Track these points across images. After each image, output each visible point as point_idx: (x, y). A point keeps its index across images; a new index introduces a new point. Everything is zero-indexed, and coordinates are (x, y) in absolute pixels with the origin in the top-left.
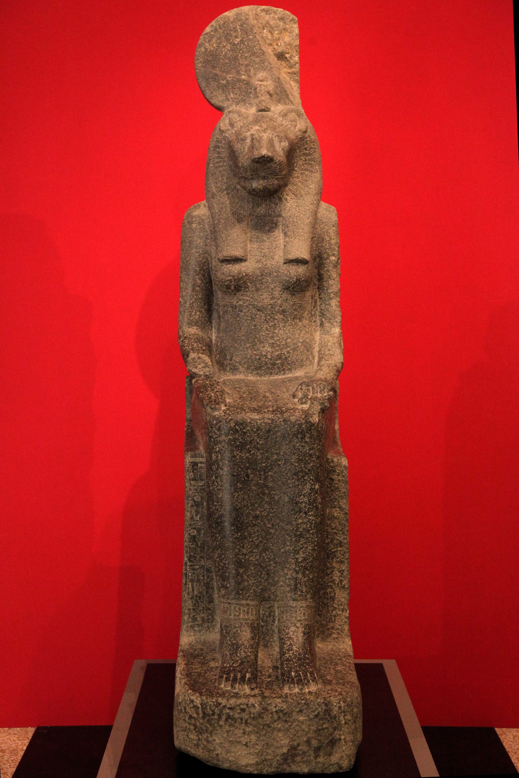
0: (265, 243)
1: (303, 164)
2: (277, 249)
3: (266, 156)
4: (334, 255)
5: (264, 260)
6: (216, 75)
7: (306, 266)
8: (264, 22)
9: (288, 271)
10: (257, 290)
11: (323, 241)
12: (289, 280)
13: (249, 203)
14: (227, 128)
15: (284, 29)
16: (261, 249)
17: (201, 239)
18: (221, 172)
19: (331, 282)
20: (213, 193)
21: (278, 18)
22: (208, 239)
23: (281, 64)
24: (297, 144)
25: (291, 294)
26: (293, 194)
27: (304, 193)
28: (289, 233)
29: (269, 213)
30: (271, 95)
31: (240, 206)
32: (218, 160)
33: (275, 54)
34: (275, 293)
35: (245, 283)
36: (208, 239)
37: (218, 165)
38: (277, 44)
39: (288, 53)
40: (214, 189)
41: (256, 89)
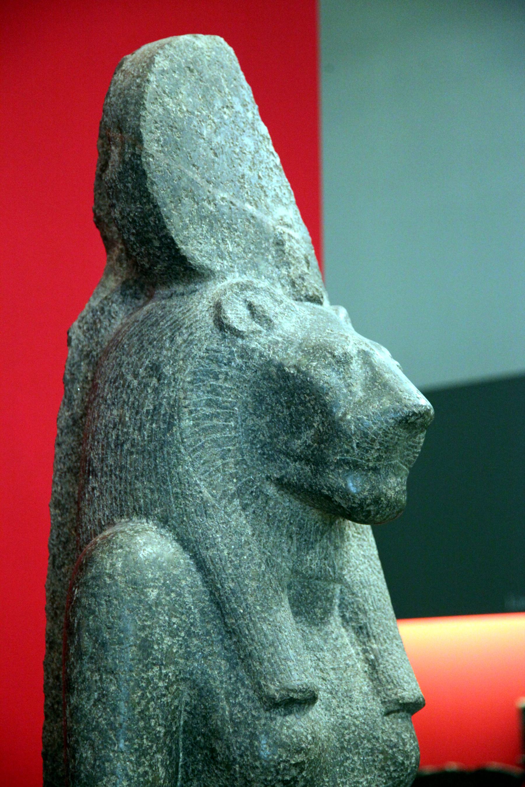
13: (291, 537)
17: (173, 634)
18: (219, 446)
20: (204, 502)
22: (197, 636)
28: (374, 629)
29: (325, 571)
31: (274, 545)
32: (208, 411)
36: (197, 636)
37: (208, 423)
40: (204, 490)
41: (279, 243)
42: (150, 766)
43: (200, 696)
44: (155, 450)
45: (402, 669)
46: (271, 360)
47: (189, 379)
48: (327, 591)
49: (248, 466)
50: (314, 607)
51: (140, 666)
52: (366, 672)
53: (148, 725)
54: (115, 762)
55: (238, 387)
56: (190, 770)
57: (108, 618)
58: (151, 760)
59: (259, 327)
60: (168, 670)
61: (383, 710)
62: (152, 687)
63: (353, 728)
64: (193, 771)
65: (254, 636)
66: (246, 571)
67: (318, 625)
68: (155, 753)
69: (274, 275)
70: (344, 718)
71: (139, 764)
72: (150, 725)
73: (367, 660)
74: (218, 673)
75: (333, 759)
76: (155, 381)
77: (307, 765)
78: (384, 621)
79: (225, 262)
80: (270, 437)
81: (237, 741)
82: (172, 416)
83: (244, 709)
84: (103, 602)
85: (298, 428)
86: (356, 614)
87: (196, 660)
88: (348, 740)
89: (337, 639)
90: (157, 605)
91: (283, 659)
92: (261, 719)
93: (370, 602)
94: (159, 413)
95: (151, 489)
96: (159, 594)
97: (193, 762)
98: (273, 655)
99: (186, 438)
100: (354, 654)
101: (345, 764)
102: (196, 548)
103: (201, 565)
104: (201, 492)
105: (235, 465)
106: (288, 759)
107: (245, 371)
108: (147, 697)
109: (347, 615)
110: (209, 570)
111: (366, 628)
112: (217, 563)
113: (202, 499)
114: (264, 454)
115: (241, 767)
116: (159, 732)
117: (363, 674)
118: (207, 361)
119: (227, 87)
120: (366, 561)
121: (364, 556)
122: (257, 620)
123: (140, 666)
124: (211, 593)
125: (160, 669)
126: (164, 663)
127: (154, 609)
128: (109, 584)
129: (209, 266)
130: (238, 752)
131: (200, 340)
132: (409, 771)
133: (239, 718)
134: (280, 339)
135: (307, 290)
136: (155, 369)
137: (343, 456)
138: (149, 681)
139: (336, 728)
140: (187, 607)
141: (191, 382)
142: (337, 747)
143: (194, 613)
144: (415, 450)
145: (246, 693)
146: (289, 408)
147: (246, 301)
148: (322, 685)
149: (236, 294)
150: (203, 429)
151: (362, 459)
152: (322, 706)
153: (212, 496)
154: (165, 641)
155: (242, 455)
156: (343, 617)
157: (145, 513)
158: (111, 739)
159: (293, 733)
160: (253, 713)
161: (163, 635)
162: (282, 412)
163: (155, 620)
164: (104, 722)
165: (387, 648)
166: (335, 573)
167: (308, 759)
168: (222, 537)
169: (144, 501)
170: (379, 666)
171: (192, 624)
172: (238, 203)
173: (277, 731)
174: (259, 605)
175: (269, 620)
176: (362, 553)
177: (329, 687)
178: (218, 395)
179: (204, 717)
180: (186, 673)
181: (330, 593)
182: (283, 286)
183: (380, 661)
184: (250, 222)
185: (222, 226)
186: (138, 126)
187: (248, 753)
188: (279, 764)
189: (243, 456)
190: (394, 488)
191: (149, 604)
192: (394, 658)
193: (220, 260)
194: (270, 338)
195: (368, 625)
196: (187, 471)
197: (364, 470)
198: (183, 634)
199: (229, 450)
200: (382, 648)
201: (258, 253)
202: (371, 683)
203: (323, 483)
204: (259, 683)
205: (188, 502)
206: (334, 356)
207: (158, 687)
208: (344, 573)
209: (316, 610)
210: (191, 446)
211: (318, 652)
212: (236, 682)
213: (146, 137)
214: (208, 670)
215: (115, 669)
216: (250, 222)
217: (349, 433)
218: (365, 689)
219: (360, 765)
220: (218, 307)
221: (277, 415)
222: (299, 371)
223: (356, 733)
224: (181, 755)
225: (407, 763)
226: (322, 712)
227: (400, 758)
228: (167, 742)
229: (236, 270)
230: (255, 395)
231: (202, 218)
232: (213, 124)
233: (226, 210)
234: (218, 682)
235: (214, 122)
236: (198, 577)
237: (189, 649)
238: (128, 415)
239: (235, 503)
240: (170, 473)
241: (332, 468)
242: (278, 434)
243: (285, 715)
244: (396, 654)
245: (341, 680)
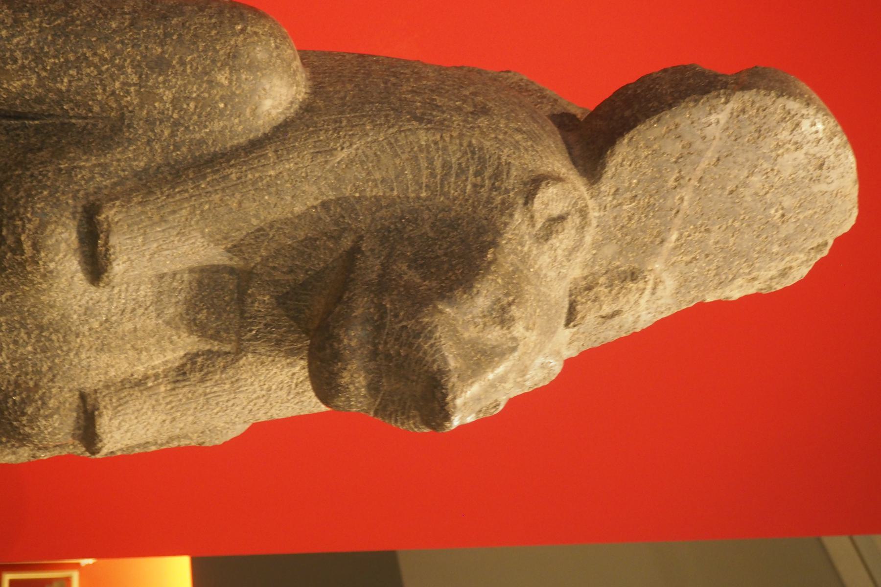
2: (131, 353)
5: (96, 325)
9: (57, 410)
12: (24, 414)
13: (291, 271)
14: (537, 215)
17: (175, 101)
18: (397, 177)
20: (331, 152)
22: (173, 135)
27: (302, 399)
29: (251, 324)
32: (438, 163)
41: (634, 275)
42: (23, 67)
43: (104, 138)
44: (389, 103)
45: (136, 421)
46: (501, 235)
47: (474, 141)
48: (227, 330)
49: (374, 213)
50: (208, 308)
51: (138, 58)
52: (132, 375)
53: (70, 65)
54: (29, 23)
55: (467, 200)
56: (18, 132)
57: (196, 24)
58: (30, 69)
59: (539, 225)
60: (133, 94)
61: (87, 391)
62: (114, 72)
63: (65, 349)
64: (18, 135)
65: (173, 197)
66: (250, 196)
67: (188, 314)
68: (39, 75)
69: (597, 267)
70: (77, 336)
71: (26, 51)
72: (70, 68)
73: (146, 377)
74: (129, 158)
75: (28, 311)
76: (471, 109)
77: (18, 257)
78: (194, 405)
80: (409, 238)
81: (49, 171)
82: (430, 122)
83: (87, 182)
84: (213, 21)
85: (422, 265)
86: (201, 370)
87: (145, 132)
89: (171, 342)
90: (210, 82)
91: (145, 231)
92: (75, 200)
93: (216, 389)
94: (434, 110)
95: (345, 97)
96: (222, 86)
97: (28, 135)
98: (150, 218)
99: (406, 136)
100: (153, 364)
101: (22, 330)
102: (276, 140)
103: (256, 145)
104: (343, 149)
105: (375, 197)
106: (27, 231)
107: (486, 207)
108: (103, 65)
109: (200, 360)
110: (251, 152)
111: (184, 380)
112: (259, 161)
113: (336, 149)
114: (389, 232)
115: (18, 176)
116: (62, 82)
117: (130, 371)
118: (496, 163)
119: (805, 217)
120: (264, 392)
121: (269, 390)
122: (192, 203)
123: (138, 58)
124: (223, 155)
125: (135, 85)
126: (142, 90)
127: (205, 79)
128: (234, 28)
129: (605, 176)
130: (36, 172)
131: (519, 157)
132: (15, 423)
133: (76, 176)
134: (526, 249)
135: (582, 303)
136: (485, 111)
137: (391, 311)
138: (121, 68)
139: (65, 321)
140: (207, 123)
141: (470, 144)
142: (43, 318)
143: (200, 131)
144: (399, 414)
145: (106, 187)
146: (445, 255)
147: (568, 214)
148: (116, 307)
149: (576, 203)
150: (417, 157)
151: (388, 334)
152: (91, 302)
153: (339, 163)
154: (167, 92)
155: (388, 206)
156: (197, 355)
157: (317, 89)
158: (55, 20)
159: (57, 241)
160: (82, 193)
161: (174, 90)
162: (439, 249)
163: (192, 79)
164: (75, 14)
165: (160, 404)
166: (249, 340)
167: (26, 261)
168: (289, 169)
169: (330, 92)
170: (141, 391)
171: (187, 128)
172: (678, 221)
173: (60, 219)
174: (209, 209)
175: (191, 219)
176: (274, 387)
177: (114, 318)
178: (457, 175)
179: (79, 142)
180: (130, 119)
181: (225, 335)
182: (585, 278)
183: (145, 393)
184: (656, 237)
185: (651, 196)
186: (759, 88)
187: (35, 183)
188: (21, 219)
189: (386, 207)
190: (352, 383)
191: (210, 71)
192: (149, 413)
193: (613, 190)
194: (527, 237)
195: (187, 383)
196: (367, 134)
197: (375, 338)
198: (175, 116)
199: (392, 190)
200: (160, 397)
202: (119, 380)
203: (356, 292)
204: (117, 198)
205: (331, 132)
206: (510, 304)
207: (114, 81)
208: (250, 355)
210: (397, 140)
211: (156, 310)
212: (119, 176)
213: (748, 96)
214: (134, 147)
215: (135, 28)
216: (656, 237)
217: (419, 316)
218: (112, 373)
219: (22, 354)
220: (558, 179)
221: (436, 244)
222: (490, 263)
223: (59, 352)
224: (37, 122)
225: (24, 420)
226: (83, 302)
227: (30, 410)
228: (50, 95)
229: (602, 213)
230: (459, 219)
232: (764, 191)
233: (669, 203)
234: (119, 156)
235: (766, 193)
236: (243, 140)
237: (158, 123)
238: (429, 83)
239: (330, 193)
240: (364, 116)
241: (375, 300)
242: (413, 246)
243: (79, 232)
244: (153, 418)
245: (122, 339)
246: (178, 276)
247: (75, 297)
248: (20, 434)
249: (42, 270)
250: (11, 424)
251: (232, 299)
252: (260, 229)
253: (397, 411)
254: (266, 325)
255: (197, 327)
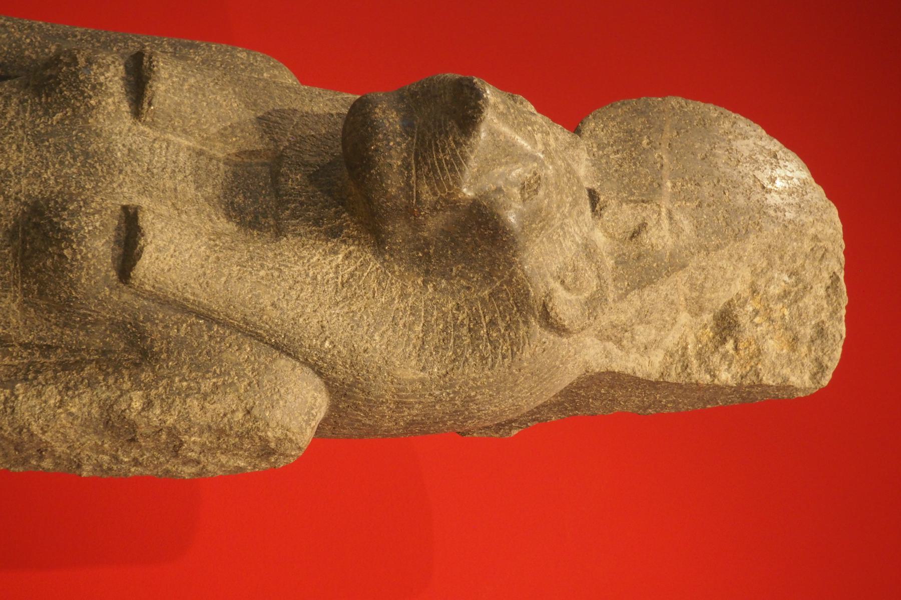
0: (193, 186)
1: (444, 313)
3: (480, 102)
4: (149, 405)
5: (138, 170)
6: (661, 130)
7: (113, 274)
8: (808, 276)
10: (38, 139)
11: (198, 368)
15: (795, 339)
16: (174, 171)
19: (52, 395)
21: (823, 322)
23: (705, 326)
24: (509, 283)
25: (16, 225)
26: (352, 275)
27: (354, 308)
29: (288, 202)
30: (635, 234)
33: (729, 303)
34: (24, 182)
35: (64, 103)
38: (756, 312)
39: (736, 348)
67: (225, 198)
70: (121, 172)
75: (76, 135)
79: (595, 150)
88: (96, 163)
89: (211, 220)
132: (55, 220)
167: (78, 70)
172: (665, 172)
201: (622, 183)
209: (241, 196)
219: (67, 173)
231: (630, 132)
243: (126, 67)
246: (215, 162)
247: (120, 133)
248: (59, 230)
249: (93, 81)
250: (51, 221)
251: (266, 184)
252: (284, 111)
253: (434, 134)
254: (302, 204)
255: (234, 211)
